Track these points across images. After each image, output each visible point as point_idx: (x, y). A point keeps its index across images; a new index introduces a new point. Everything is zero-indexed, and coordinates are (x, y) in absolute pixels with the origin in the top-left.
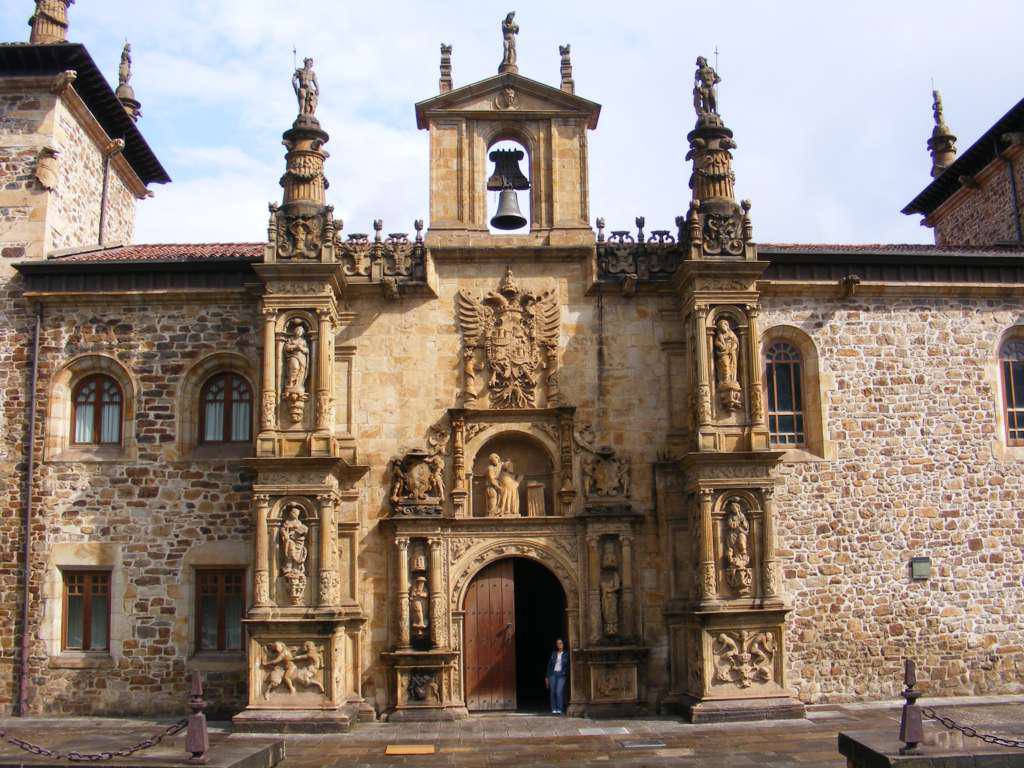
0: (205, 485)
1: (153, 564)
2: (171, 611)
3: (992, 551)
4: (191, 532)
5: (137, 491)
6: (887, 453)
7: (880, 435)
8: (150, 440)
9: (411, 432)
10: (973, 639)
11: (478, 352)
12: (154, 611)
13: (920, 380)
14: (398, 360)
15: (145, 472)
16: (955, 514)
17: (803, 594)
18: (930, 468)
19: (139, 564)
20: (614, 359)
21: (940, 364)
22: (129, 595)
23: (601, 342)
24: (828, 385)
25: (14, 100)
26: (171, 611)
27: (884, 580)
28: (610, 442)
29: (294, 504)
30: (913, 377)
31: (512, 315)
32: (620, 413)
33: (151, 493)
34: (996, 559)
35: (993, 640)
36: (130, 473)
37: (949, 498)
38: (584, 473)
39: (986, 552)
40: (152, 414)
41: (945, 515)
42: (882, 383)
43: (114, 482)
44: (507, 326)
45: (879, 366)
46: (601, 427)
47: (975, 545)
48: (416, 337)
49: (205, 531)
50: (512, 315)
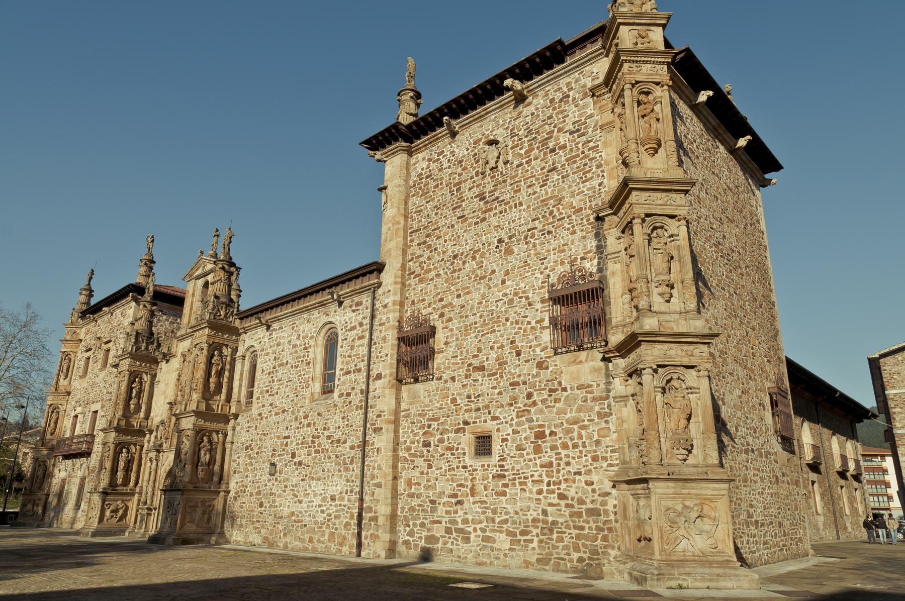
16: (288, 437)
21: (296, 352)
30: (285, 361)
34: (300, 463)
41: (285, 438)
45: (275, 359)
47: (293, 455)
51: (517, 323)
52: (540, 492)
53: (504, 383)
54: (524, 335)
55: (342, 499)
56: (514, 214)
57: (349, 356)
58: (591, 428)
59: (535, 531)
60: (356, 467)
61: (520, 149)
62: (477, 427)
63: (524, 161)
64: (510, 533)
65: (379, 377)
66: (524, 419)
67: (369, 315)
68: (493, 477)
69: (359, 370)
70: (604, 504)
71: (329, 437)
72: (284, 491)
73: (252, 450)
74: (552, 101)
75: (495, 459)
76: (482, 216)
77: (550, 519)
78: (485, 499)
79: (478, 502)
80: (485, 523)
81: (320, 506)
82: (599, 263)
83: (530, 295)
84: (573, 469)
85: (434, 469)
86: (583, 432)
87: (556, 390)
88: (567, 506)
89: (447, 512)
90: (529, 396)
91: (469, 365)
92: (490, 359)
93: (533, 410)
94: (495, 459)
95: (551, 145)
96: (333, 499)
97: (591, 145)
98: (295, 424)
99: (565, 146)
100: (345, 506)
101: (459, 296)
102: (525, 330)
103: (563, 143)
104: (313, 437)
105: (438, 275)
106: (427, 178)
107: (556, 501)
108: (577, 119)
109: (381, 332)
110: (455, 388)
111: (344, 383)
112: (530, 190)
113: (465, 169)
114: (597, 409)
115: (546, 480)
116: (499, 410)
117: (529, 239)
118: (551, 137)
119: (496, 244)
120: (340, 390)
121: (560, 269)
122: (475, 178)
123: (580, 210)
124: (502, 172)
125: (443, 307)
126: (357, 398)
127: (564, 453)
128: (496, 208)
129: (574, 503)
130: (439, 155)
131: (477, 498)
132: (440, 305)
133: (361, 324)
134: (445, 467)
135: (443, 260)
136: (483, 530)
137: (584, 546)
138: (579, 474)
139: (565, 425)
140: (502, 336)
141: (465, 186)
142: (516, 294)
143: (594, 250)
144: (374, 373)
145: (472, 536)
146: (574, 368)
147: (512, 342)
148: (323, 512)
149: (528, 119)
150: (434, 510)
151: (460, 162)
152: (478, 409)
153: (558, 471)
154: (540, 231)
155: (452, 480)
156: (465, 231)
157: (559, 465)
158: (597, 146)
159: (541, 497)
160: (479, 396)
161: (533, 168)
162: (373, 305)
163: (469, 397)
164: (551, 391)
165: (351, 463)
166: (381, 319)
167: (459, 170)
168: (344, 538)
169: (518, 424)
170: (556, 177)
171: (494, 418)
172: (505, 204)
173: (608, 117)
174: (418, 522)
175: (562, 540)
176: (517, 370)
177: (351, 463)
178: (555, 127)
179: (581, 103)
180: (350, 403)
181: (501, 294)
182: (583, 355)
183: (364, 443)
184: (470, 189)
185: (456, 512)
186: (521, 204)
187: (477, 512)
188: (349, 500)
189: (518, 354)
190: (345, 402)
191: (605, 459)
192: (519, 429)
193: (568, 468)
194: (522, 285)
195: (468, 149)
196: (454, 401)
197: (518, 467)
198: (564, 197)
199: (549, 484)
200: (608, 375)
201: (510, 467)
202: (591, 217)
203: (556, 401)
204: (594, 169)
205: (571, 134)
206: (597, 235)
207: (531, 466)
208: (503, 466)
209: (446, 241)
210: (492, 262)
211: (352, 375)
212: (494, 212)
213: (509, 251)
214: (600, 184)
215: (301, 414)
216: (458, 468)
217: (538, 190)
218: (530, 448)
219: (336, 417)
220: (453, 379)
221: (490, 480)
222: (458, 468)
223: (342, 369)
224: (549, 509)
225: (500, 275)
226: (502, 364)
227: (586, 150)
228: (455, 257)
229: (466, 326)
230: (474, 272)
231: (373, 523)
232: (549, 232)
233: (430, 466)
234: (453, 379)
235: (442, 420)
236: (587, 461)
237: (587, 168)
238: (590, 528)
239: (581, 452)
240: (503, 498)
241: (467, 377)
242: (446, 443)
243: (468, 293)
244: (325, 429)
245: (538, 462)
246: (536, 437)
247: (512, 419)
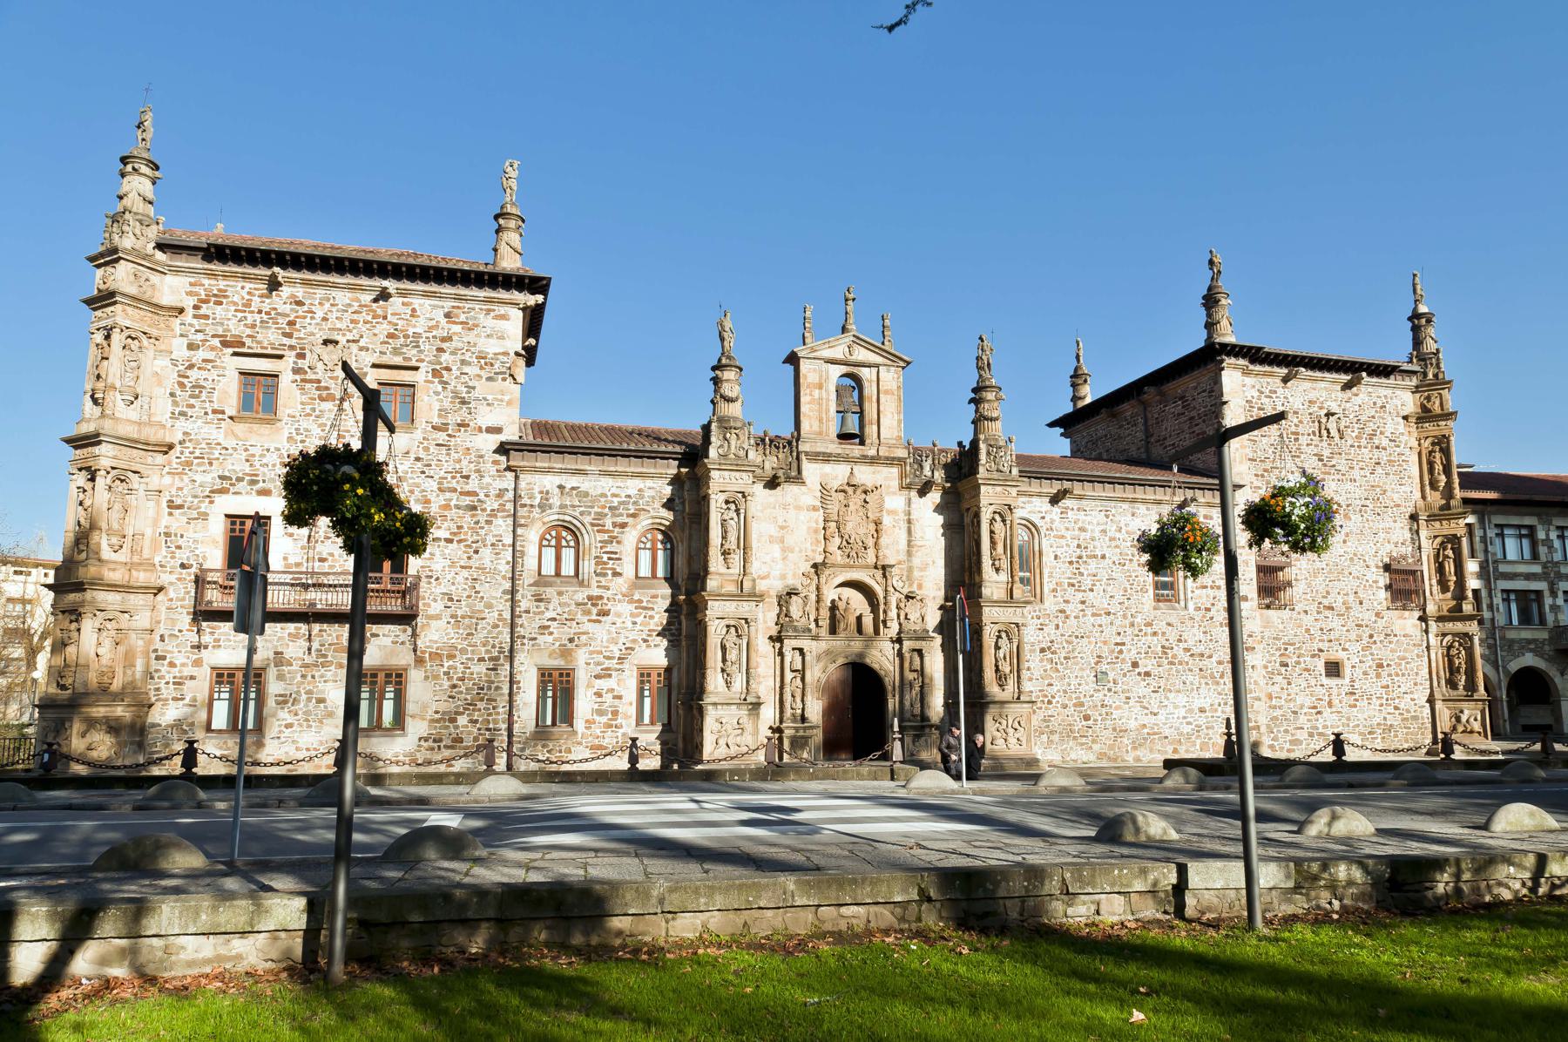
0: (645, 608)
1: (607, 664)
2: (620, 697)
4: (634, 641)
5: (595, 611)
6: (1083, 602)
8: (605, 575)
9: (790, 576)
10: (1132, 724)
11: (832, 526)
12: (608, 698)
13: (1103, 557)
14: (782, 528)
15: (601, 598)
18: (1108, 614)
19: (598, 664)
20: (917, 533)
22: (589, 686)
23: (909, 522)
24: (1048, 559)
25: (489, 311)
26: (620, 697)
28: (915, 588)
29: (732, 623)
31: (856, 500)
32: (922, 570)
33: (605, 613)
34: (1147, 674)
36: (590, 598)
38: (898, 608)
39: (1141, 669)
40: (605, 557)
43: (578, 604)
44: (852, 507)
45: (1079, 546)
46: (909, 578)
48: (792, 512)
49: (645, 641)
50: (856, 500)
53: (1351, 624)
56: (1349, 486)
71: (1187, 650)
84: (1403, 689)
90: (1371, 636)
92: (1338, 605)
94: (1347, 680)
96: (1202, 710)
98: (1129, 630)
110: (1308, 620)
134: (1304, 684)
141: (1303, 440)
150: (1296, 719)
177: (1222, 676)
196: (1308, 630)
207: (1371, 685)
218: (1372, 674)
219: (1195, 630)
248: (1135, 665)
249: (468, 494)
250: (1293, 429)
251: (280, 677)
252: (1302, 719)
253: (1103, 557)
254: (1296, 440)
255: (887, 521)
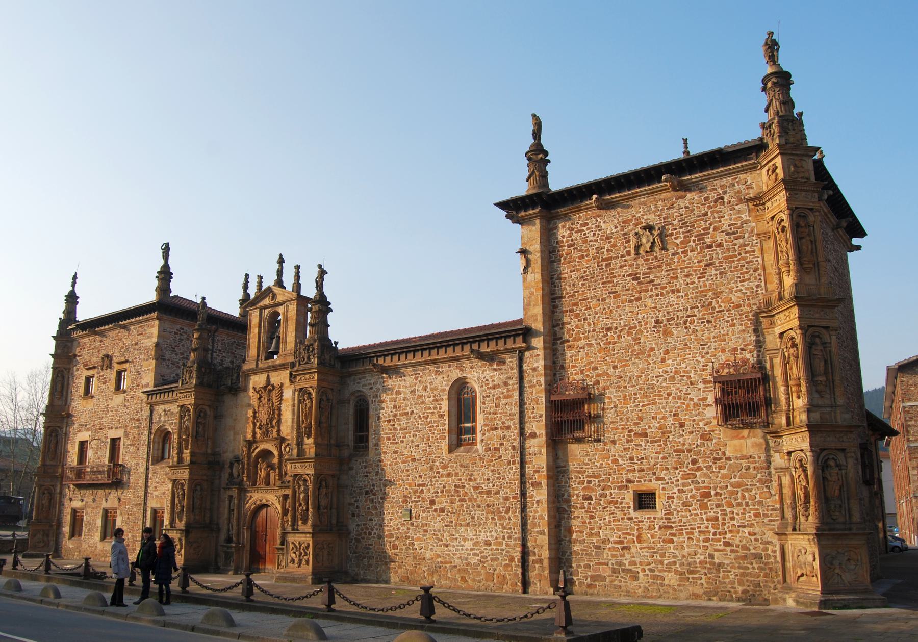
3: (440, 506)
7: (392, 443)
13: (412, 412)
16: (424, 485)
17: (358, 525)
21: (423, 403)
27: (391, 520)
30: (409, 411)
34: (442, 510)
35: (439, 556)
37: (421, 477)
41: (419, 485)
42: (395, 416)
45: (395, 407)
47: (432, 502)
51: (680, 398)
52: (707, 540)
53: (669, 449)
54: (686, 410)
55: (500, 544)
56: (672, 299)
57: (495, 413)
58: (754, 491)
59: (703, 571)
60: (515, 518)
61: (676, 238)
62: (642, 485)
63: (680, 251)
64: (676, 572)
65: (533, 435)
66: (689, 481)
67: (516, 375)
68: (660, 528)
69: (508, 428)
70: (766, 549)
71: (476, 488)
72: (424, 535)
73: (375, 494)
74: (706, 199)
75: (660, 510)
76: (637, 295)
77: (716, 561)
78: (653, 545)
79: (644, 548)
80: (653, 565)
81: (472, 550)
82: (758, 356)
83: (692, 375)
85: (597, 519)
86: (746, 494)
87: (720, 459)
88: (732, 551)
89: (613, 556)
90: (694, 462)
91: (630, 431)
92: (653, 428)
93: (698, 474)
95: (708, 241)
96: (488, 543)
97: (748, 248)
99: (720, 245)
100: (503, 550)
101: (615, 367)
102: (688, 406)
103: (719, 241)
104: (456, 486)
105: (590, 345)
106: (569, 246)
107: (722, 547)
108: (733, 222)
109: (532, 393)
111: (490, 439)
112: (688, 280)
113: (614, 246)
114: (759, 476)
115: (713, 531)
116: (664, 472)
117: (688, 324)
118: (709, 233)
119: (653, 324)
120: (486, 445)
121: (723, 358)
122: (627, 258)
123: (739, 306)
124: (656, 258)
125: (598, 375)
126: (507, 454)
127: (728, 510)
128: (651, 290)
129: (739, 549)
130: (582, 225)
131: (645, 545)
132: (594, 373)
133: (506, 384)
135: (594, 330)
136: (650, 570)
137: (747, 581)
138: (744, 527)
139: (729, 488)
140: (664, 408)
142: (676, 373)
143: (754, 344)
144: (528, 432)
145: (641, 575)
146: (736, 442)
147: (675, 415)
148: (475, 554)
149: (683, 211)
151: (608, 238)
152: (641, 470)
153: (724, 524)
154: (699, 319)
155: (618, 530)
156: (618, 307)
157: (724, 519)
158: (754, 251)
159: (707, 544)
160: (642, 459)
161: (690, 259)
162: (521, 367)
163: (632, 459)
164: (715, 459)
165: (507, 512)
166: (530, 381)
167: (607, 246)
168: (504, 577)
169: (684, 485)
170: (714, 272)
171: (658, 479)
172: (661, 288)
173: (763, 226)
174: (582, 564)
175: (728, 577)
176: (681, 440)
178: (710, 224)
179: (737, 207)
180: (500, 457)
181: (661, 371)
182: (745, 432)
183: (523, 494)
184: (621, 267)
185: (623, 556)
186: (678, 291)
187: (644, 556)
188: (507, 545)
189: (682, 425)
190: (493, 456)
191: (766, 516)
192: (685, 489)
193: (732, 522)
194: (683, 365)
195: (616, 227)
196: (615, 461)
197: (684, 520)
198: (722, 292)
199: (715, 534)
200: (767, 449)
201: (677, 520)
202: (750, 314)
203: (720, 468)
204: (752, 272)
205: (727, 234)
206: (756, 331)
207: (698, 519)
208: (670, 519)
209: (596, 313)
210: (649, 340)
211: (500, 432)
212: (651, 293)
213: (667, 333)
214: (757, 286)
215: (437, 464)
216: (622, 519)
217: (696, 281)
218: (695, 505)
220: (614, 442)
221: (657, 529)
222: (622, 519)
223: (485, 425)
224: (716, 554)
225: (660, 354)
226: (665, 432)
227: (742, 252)
228: (609, 329)
229: (625, 396)
230: (630, 346)
231: (537, 566)
232: (709, 322)
233: (592, 517)
234: (614, 442)
235: (603, 477)
236: (750, 517)
237: (745, 270)
238: (754, 568)
239: (744, 510)
240: (671, 545)
241: (628, 441)
242: (608, 497)
243: (625, 366)
244: (470, 480)
245: (704, 516)
246: (701, 496)
247: (678, 481)
248: (432, 502)
249: (138, 420)
250: (606, 255)
251: (87, 514)
252: (607, 555)
253: (412, 412)
254: (608, 265)
255: (283, 407)
